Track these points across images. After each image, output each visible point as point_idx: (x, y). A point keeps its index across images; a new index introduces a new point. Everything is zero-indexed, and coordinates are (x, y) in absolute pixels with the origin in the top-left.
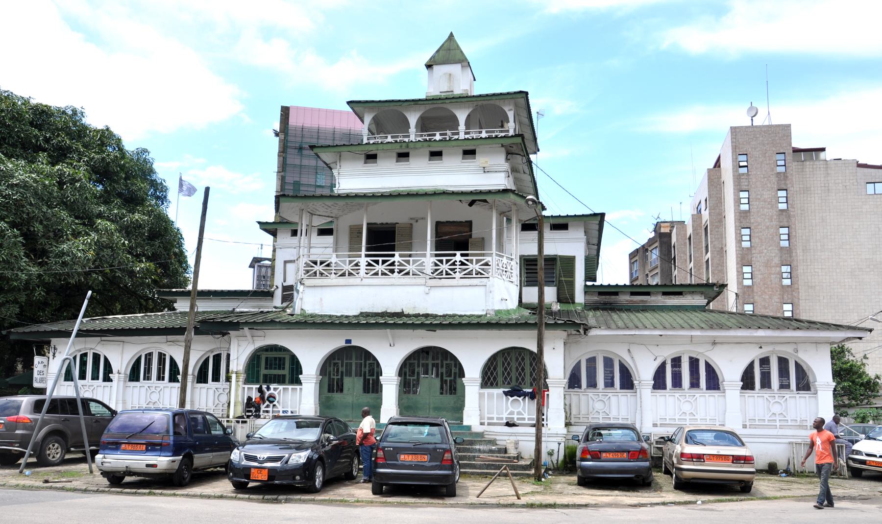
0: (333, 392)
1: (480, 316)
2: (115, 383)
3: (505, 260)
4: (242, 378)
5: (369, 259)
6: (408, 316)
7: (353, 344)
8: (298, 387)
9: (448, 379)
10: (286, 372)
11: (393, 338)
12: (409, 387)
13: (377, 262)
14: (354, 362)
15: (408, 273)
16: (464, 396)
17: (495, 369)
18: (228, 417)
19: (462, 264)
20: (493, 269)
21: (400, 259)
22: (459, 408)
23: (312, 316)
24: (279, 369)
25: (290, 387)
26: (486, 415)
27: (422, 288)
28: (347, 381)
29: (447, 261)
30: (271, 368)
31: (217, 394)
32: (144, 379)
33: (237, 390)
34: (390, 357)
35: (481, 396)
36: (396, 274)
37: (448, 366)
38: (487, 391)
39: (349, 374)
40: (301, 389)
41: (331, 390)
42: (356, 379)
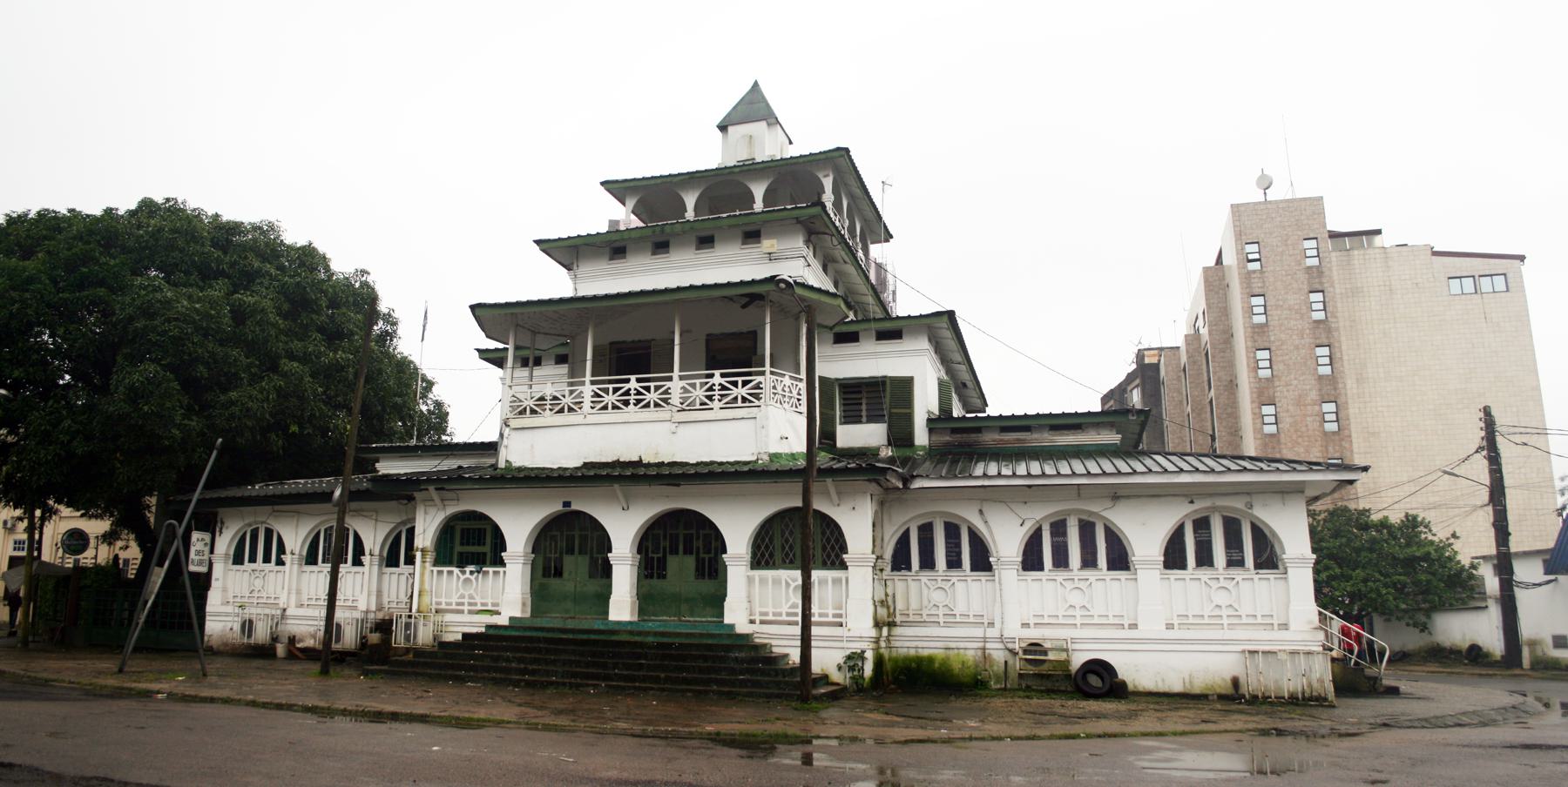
4: (430, 558)
5: (595, 387)
7: (574, 507)
10: (487, 549)
19: (723, 388)
25: (491, 570)
33: (422, 575)
34: (623, 528)
35: (750, 580)
38: (757, 573)
41: (546, 573)
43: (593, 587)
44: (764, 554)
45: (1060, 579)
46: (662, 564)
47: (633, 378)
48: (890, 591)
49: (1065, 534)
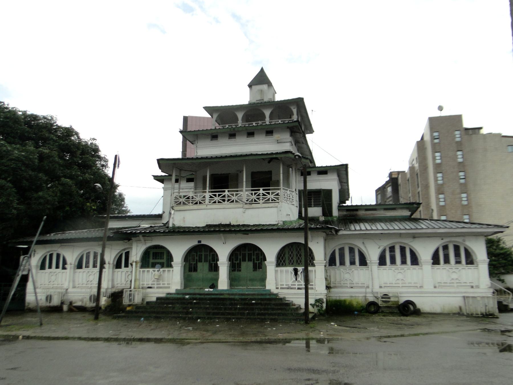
0: (192, 271)
1: (274, 225)
2: (68, 271)
3: (288, 192)
4: (139, 265)
5: (211, 194)
6: (234, 226)
7: (202, 243)
8: (171, 269)
9: (258, 262)
10: (164, 261)
11: (225, 239)
12: (235, 267)
13: (215, 195)
14: (203, 253)
15: (233, 201)
16: (266, 272)
17: (284, 255)
18: (130, 288)
19: (264, 195)
20: (281, 197)
21: (228, 193)
22: (263, 279)
23: (179, 228)
24: (161, 259)
25: (167, 269)
26: (280, 283)
27: (242, 209)
28: (200, 265)
29: (255, 194)
30: (156, 259)
31: (127, 275)
32: (86, 267)
34: (223, 250)
35: (276, 271)
36: (226, 202)
37: (257, 254)
38: (279, 269)
39: (200, 261)
40: (173, 270)
41: (190, 270)
42: (205, 263)
43: (211, 275)
44: (281, 260)
45: (393, 269)
46: (239, 265)
47: (261, 189)
48: (328, 275)
49: (394, 251)
